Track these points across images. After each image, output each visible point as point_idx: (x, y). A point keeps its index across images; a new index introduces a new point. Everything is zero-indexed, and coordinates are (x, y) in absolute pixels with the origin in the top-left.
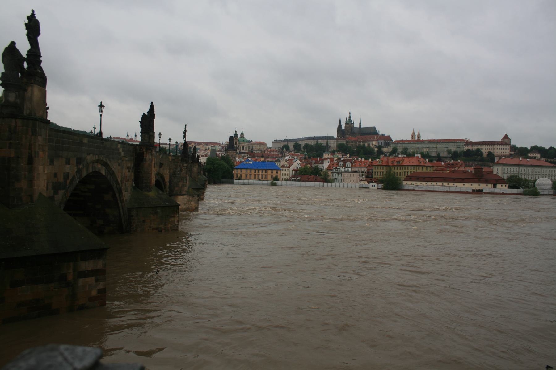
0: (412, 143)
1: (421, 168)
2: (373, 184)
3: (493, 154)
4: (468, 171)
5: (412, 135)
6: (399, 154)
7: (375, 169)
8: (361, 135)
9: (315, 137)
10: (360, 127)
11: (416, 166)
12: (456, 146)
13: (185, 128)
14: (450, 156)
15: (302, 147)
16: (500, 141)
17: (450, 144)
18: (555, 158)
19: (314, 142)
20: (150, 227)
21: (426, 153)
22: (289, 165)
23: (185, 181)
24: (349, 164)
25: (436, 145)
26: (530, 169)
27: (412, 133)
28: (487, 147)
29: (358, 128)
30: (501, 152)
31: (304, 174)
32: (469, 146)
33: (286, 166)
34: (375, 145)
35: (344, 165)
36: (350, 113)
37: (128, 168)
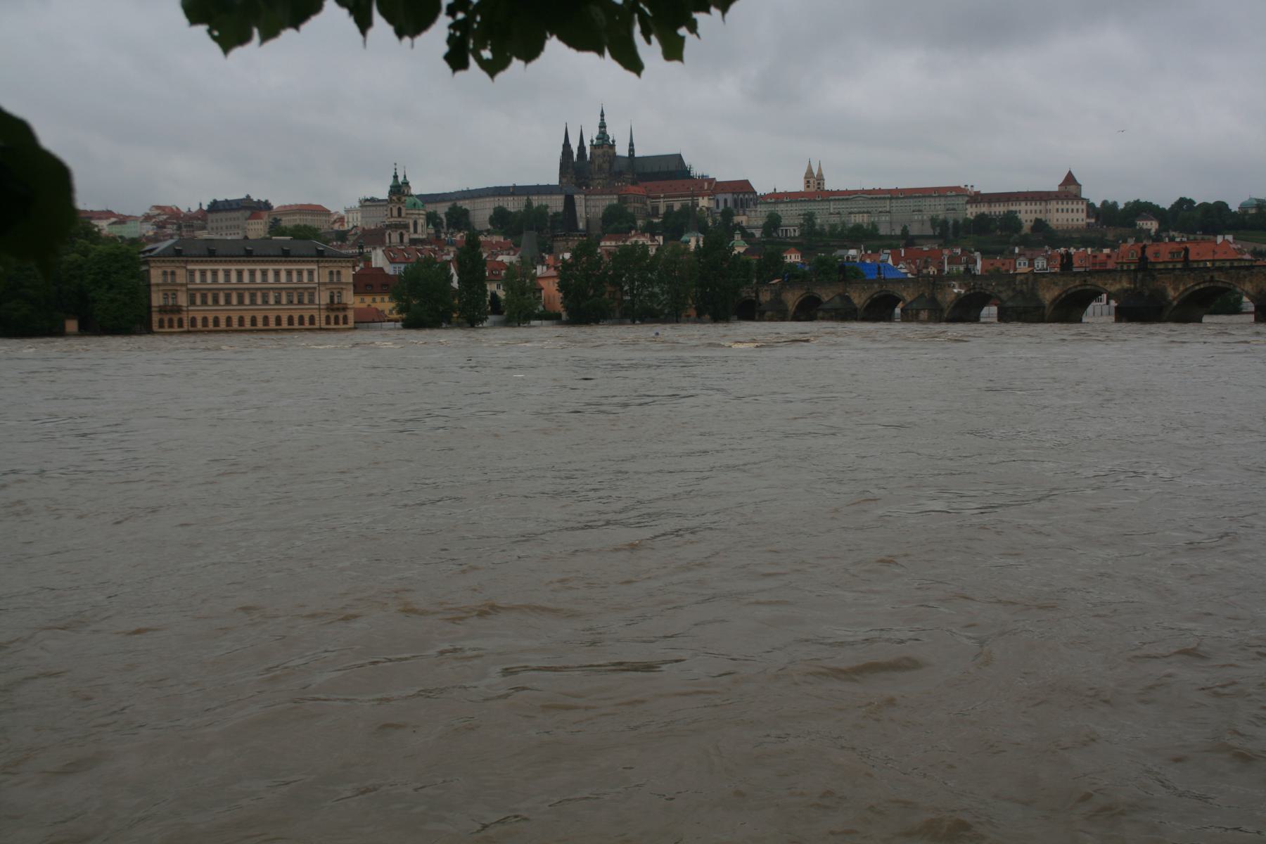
0: (820, 199)
5: (805, 178)
6: (786, 230)
9: (514, 187)
12: (945, 205)
16: (1056, 189)
17: (928, 202)
18: (1198, 233)
19: (516, 204)
21: (870, 227)
24: (1040, 262)
25: (887, 205)
27: (805, 170)
29: (624, 158)
30: (1067, 220)
34: (708, 209)
35: (1029, 264)
36: (602, 115)
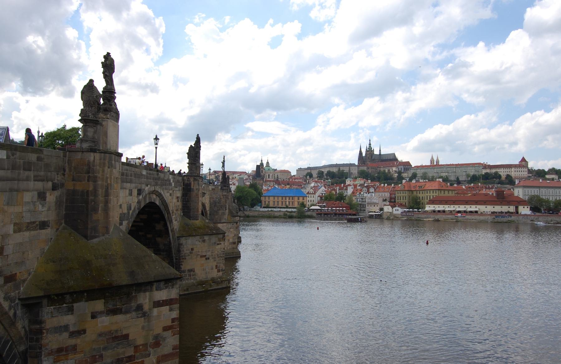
1: (443, 192)
2: (397, 208)
3: (512, 177)
4: (489, 194)
7: (398, 193)
8: (380, 162)
10: (380, 154)
11: (439, 190)
13: (224, 158)
14: (469, 180)
15: (324, 174)
16: (518, 163)
20: (198, 255)
21: (445, 177)
22: (315, 192)
23: (224, 210)
26: (551, 190)
27: (430, 158)
28: (505, 170)
31: (329, 200)
32: (487, 169)
33: (311, 192)
34: (395, 171)
36: (370, 141)
37: (177, 198)
